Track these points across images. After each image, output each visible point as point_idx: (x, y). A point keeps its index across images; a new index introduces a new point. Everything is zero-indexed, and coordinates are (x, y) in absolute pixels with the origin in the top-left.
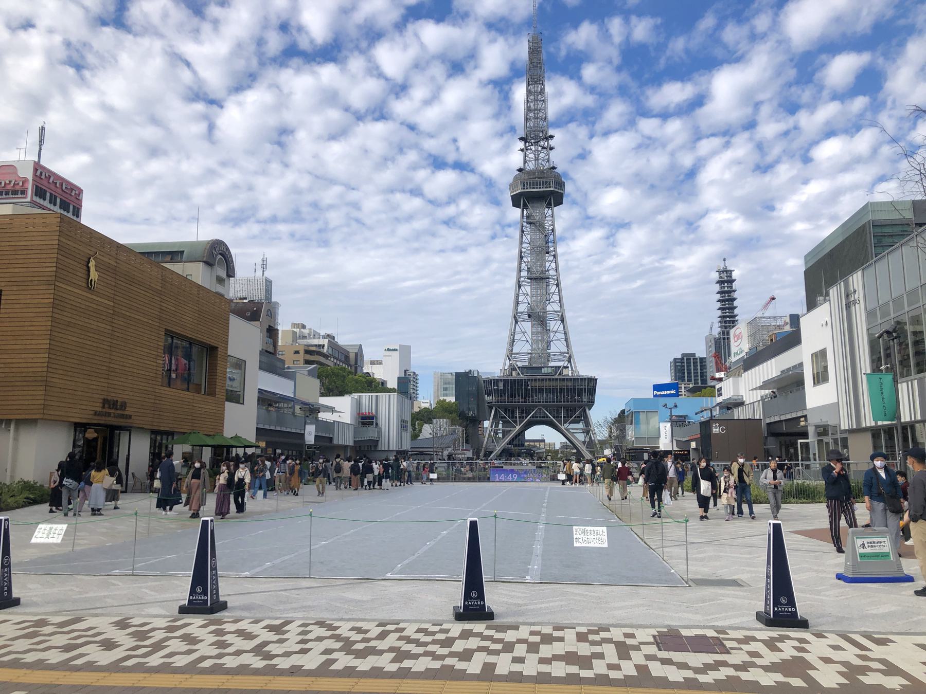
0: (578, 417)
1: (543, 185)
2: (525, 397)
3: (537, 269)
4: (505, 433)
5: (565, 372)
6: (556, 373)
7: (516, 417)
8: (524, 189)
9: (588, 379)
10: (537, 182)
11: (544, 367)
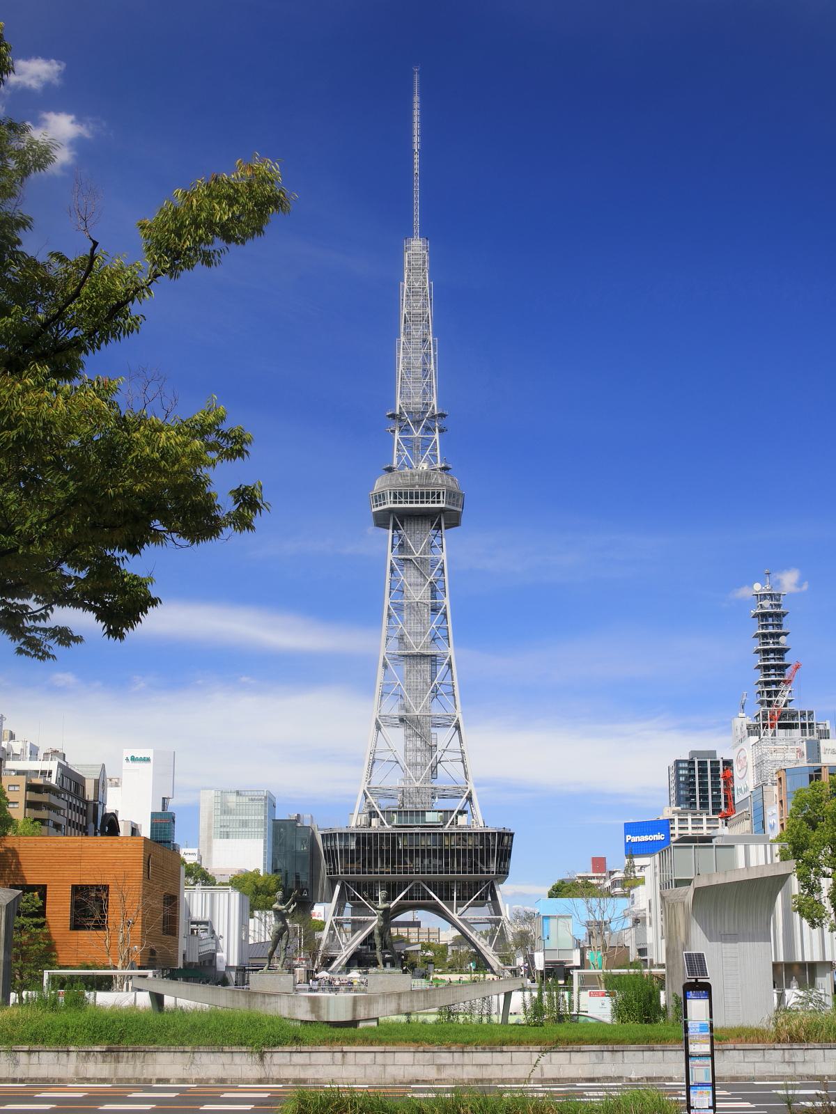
2: (393, 863)
5: (462, 820)
6: (445, 823)
8: (395, 502)
9: (499, 833)
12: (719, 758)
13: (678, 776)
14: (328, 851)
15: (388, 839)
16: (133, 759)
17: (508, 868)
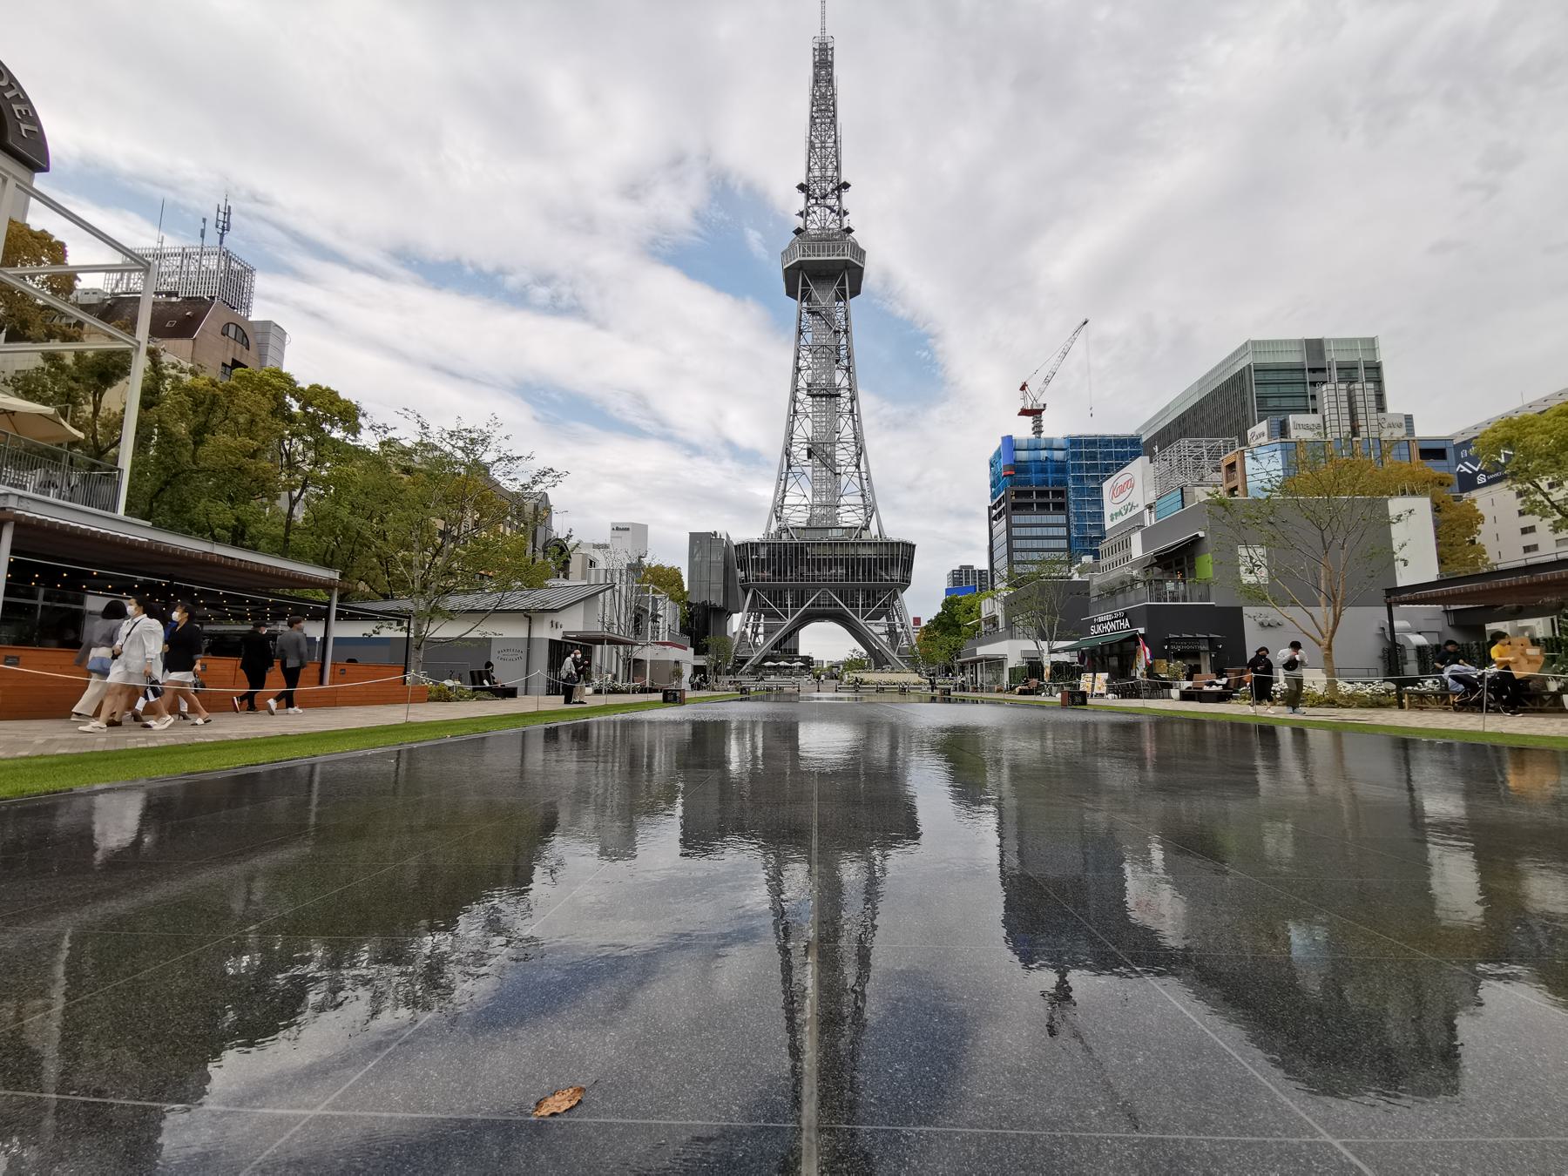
1: (834, 251)
4: (767, 633)
7: (787, 606)
8: (804, 256)
9: (903, 544)
10: (824, 247)
15: (797, 548)
16: (617, 529)
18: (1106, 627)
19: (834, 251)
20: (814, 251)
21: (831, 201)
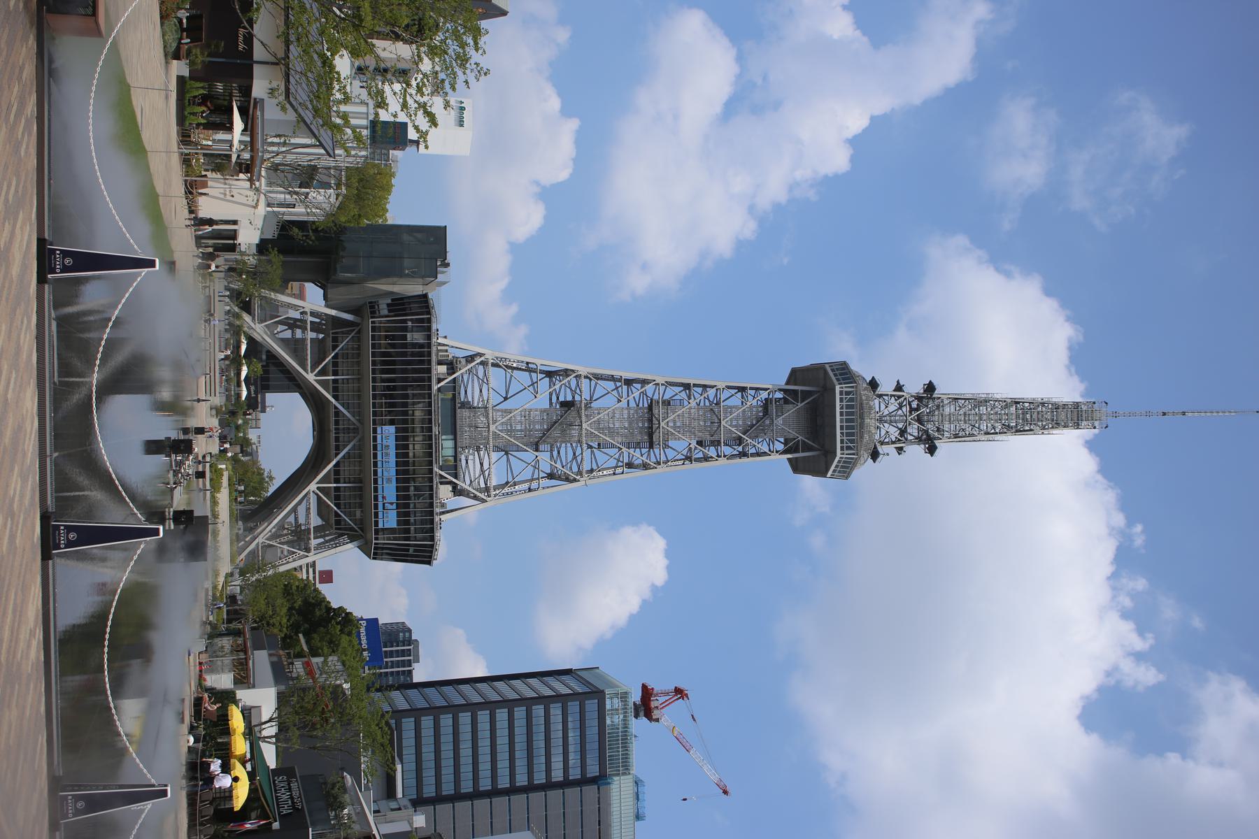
0: (338, 522)
1: (848, 434)
2: (386, 396)
3: (665, 424)
6: (441, 468)
8: (841, 393)
9: (432, 546)
10: (852, 421)
11: (455, 439)
12: (415, 665)
13: (398, 632)
14: (403, 304)
17: (382, 559)
18: (283, 791)
19: (848, 434)
20: (848, 407)
21: (913, 430)
